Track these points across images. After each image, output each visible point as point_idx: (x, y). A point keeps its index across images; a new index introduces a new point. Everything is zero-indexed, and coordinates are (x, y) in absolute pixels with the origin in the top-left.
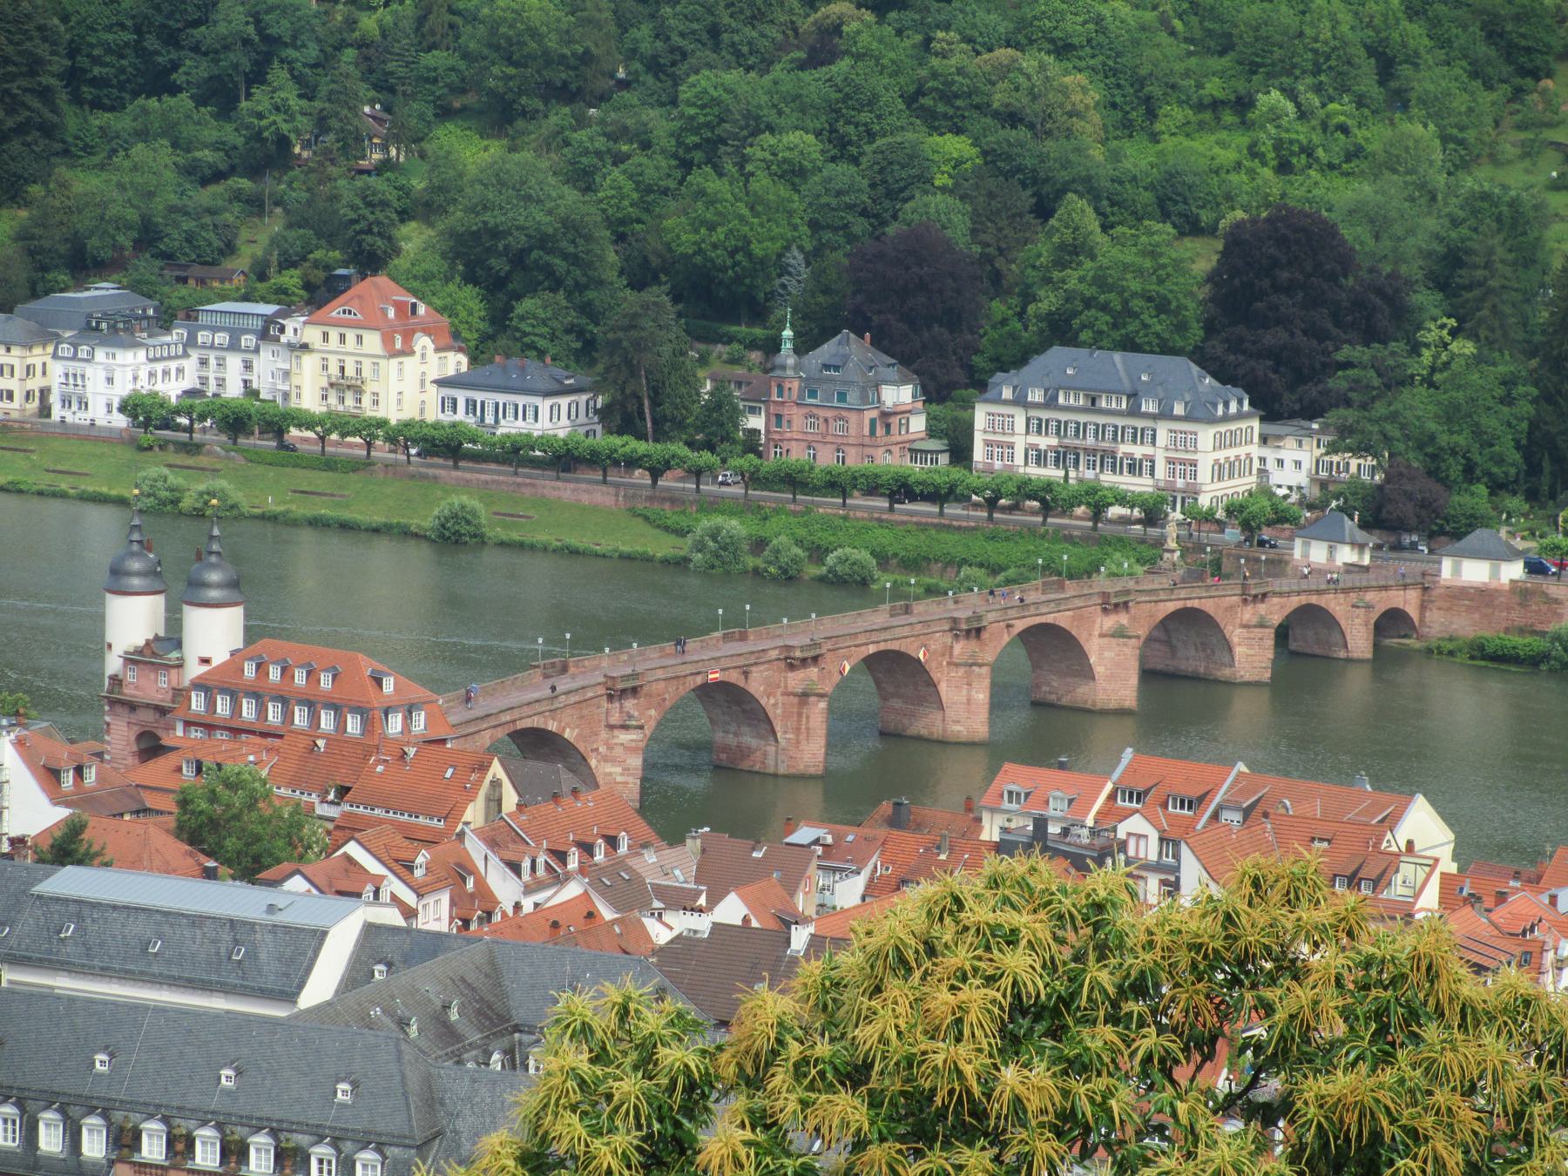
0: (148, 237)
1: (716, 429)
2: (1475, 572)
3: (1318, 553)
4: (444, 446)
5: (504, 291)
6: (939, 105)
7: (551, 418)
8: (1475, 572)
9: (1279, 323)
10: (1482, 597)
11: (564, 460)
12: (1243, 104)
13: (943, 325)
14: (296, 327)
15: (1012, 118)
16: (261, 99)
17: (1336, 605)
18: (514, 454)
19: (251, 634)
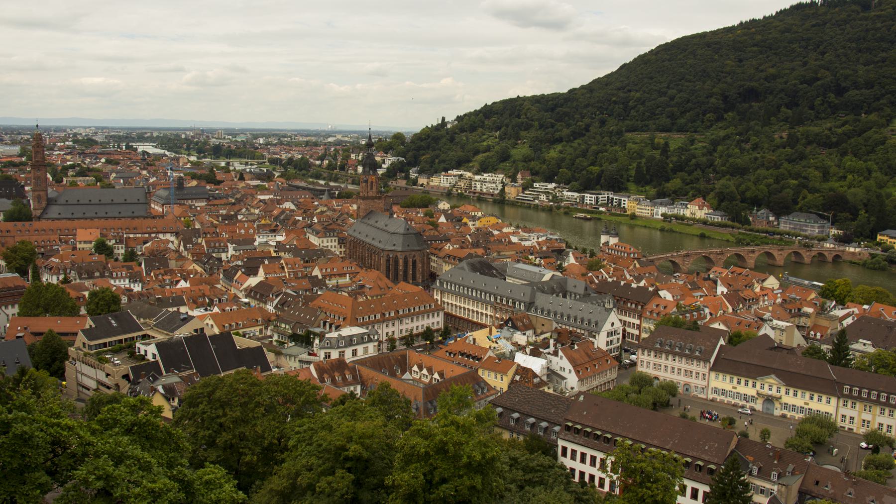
0: (675, 192)
1: (748, 222)
2: (852, 249)
3: (828, 245)
4: (705, 222)
5: (721, 202)
6: (797, 176)
7: (718, 219)
8: (852, 249)
9: (835, 209)
10: (853, 254)
11: (720, 225)
12: (845, 177)
13: (782, 209)
15: (805, 178)
16: (695, 173)
17: (826, 254)
18: (713, 224)
19: (619, 240)
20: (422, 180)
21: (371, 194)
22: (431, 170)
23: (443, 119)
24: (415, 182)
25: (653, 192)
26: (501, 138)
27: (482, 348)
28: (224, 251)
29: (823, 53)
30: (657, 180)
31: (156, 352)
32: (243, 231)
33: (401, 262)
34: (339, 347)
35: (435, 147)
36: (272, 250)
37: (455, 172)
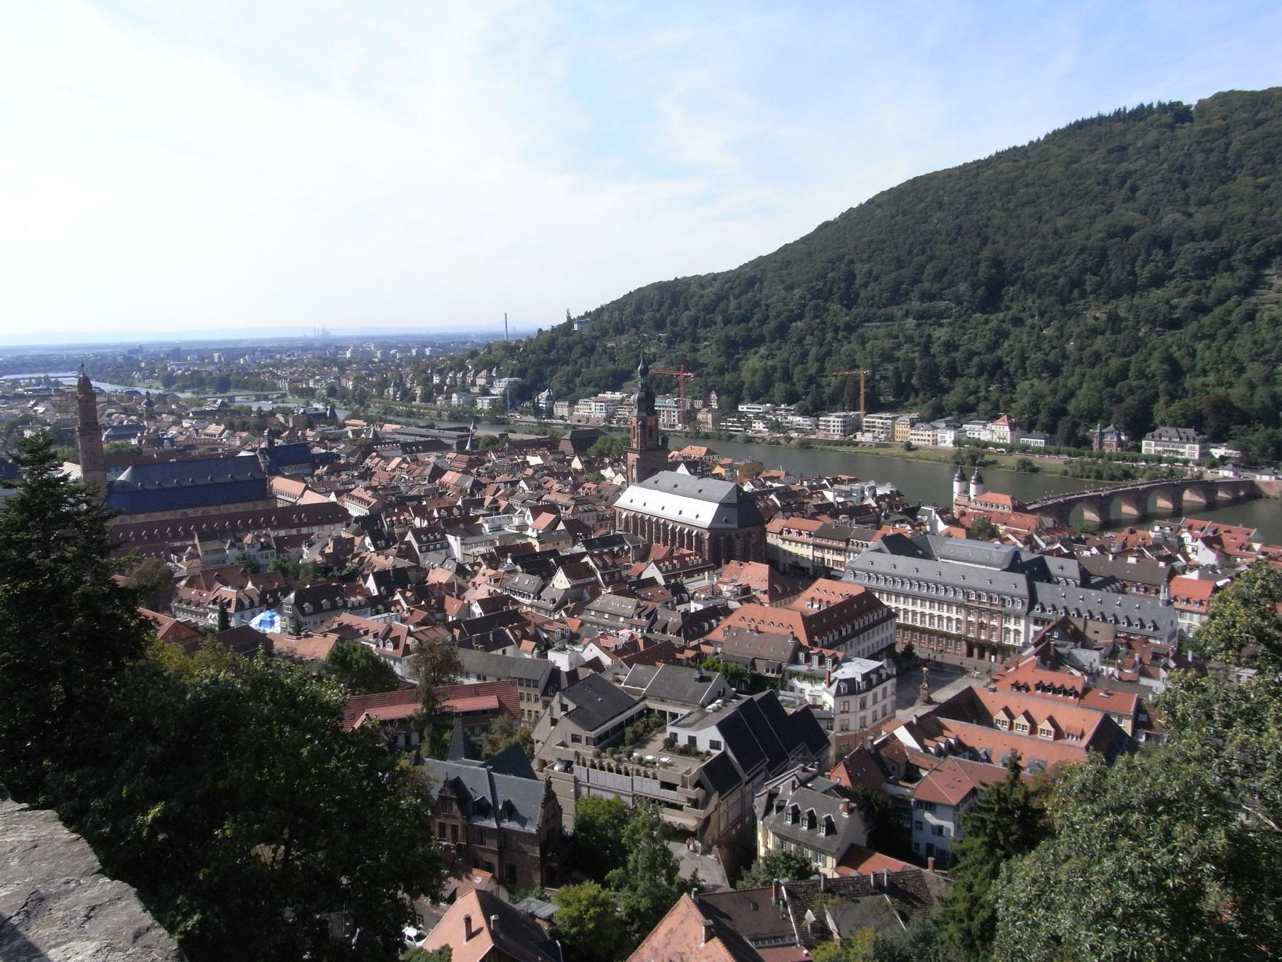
14: (990, 425)
20: (561, 409)
21: (650, 444)
22: (570, 394)
23: (569, 317)
24: (550, 413)
25: (926, 410)
26: (670, 344)
27: (846, 660)
28: (442, 548)
29: (1134, 189)
30: (927, 387)
31: (718, 737)
32: (444, 513)
33: (738, 544)
34: (860, 692)
35: (550, 361)
36: (535, 543)
37: (609, 395)
